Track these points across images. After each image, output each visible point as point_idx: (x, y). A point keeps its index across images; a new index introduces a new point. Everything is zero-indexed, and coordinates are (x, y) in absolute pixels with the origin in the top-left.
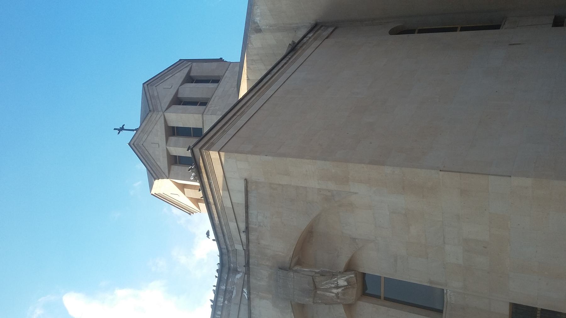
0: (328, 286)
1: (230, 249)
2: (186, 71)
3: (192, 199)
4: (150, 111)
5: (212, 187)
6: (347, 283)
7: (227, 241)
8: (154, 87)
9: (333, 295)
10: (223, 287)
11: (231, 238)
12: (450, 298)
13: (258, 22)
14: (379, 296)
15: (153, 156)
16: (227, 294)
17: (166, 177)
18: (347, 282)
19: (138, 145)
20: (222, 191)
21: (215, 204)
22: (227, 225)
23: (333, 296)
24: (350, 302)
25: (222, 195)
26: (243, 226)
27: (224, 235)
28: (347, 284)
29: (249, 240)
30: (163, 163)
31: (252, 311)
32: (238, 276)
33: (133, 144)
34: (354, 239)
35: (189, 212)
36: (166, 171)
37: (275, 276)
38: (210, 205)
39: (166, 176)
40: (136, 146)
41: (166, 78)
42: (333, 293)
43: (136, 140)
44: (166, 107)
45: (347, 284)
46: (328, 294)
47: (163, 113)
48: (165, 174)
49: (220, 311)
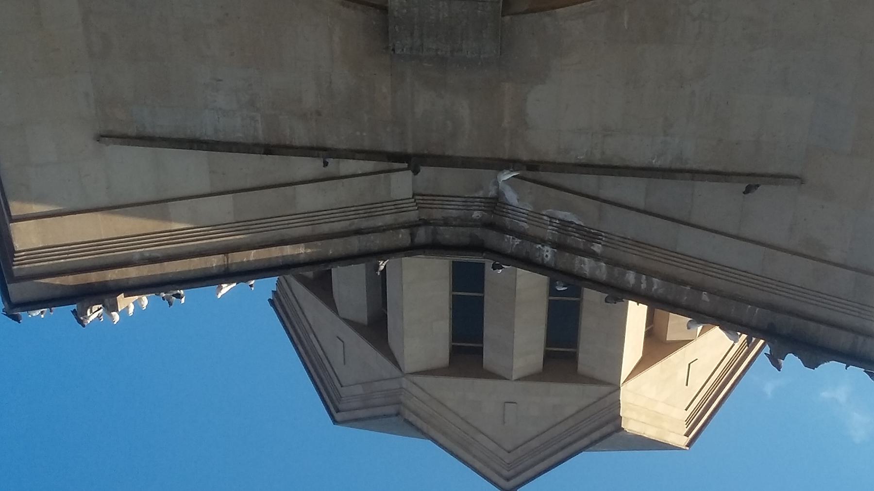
1: (413, 215)
5: (158, 255)
7: (379, 222)
20: (170, 220)
21: (226, 250)
22: (311, 216)
25: (188, 223)
26: (308, 166)
27: (358, 232)
32: (511, 196)
38: (234, 268)
49: (624, 275)
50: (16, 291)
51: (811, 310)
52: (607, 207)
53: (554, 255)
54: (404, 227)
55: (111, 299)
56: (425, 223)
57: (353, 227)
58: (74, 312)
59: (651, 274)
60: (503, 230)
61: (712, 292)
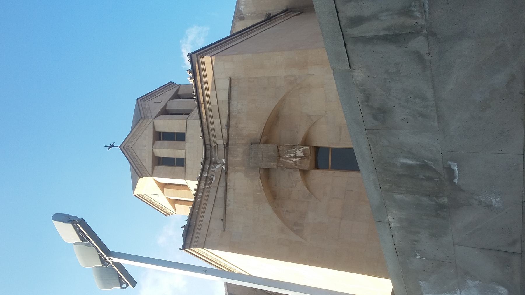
1: (213, 144)
2: (175, 90)
3: (169, 200)
4: (142, 118)
6: (304, 154)
7: (211, 137)
8: (146, 102)
9: (293, 162)
10: (205, 175)
11: (214, 135)
13: (242, 10)
15: (139, 157)
16: (208, 180)
17: (149, 176)
19: (127, 148)
21: (204, 103)
22: (212, 122)
23: (292, 163)
24: (304, 169)
26: (224, 122)
27: (209, 132)
29: (230, 126)
30: (148, 163)
31: (228, 184)
32: (218, 167)
33: (123, 147)
34: (310, 116)
35: (165, 214)
36: (150, 170)
37: (248, 151)
38: (200, 105)
39: (150, 175)
40: (126, 148)
41: (157, 95)
42: (292, 161)
43: (126, 144)
44: (156, 115)
46: (288, 161)
47: (153, 119)
48: (149, 173)
49: (201, 192)
50: (194, 56)
51: (195, 234)
53: (205, 176)
54: (210, 142)
55: (193, 78)
56: (211, 147)
57: (210, 131)
58: (190, 70)
59: (202, 198)
60: (210, 165)
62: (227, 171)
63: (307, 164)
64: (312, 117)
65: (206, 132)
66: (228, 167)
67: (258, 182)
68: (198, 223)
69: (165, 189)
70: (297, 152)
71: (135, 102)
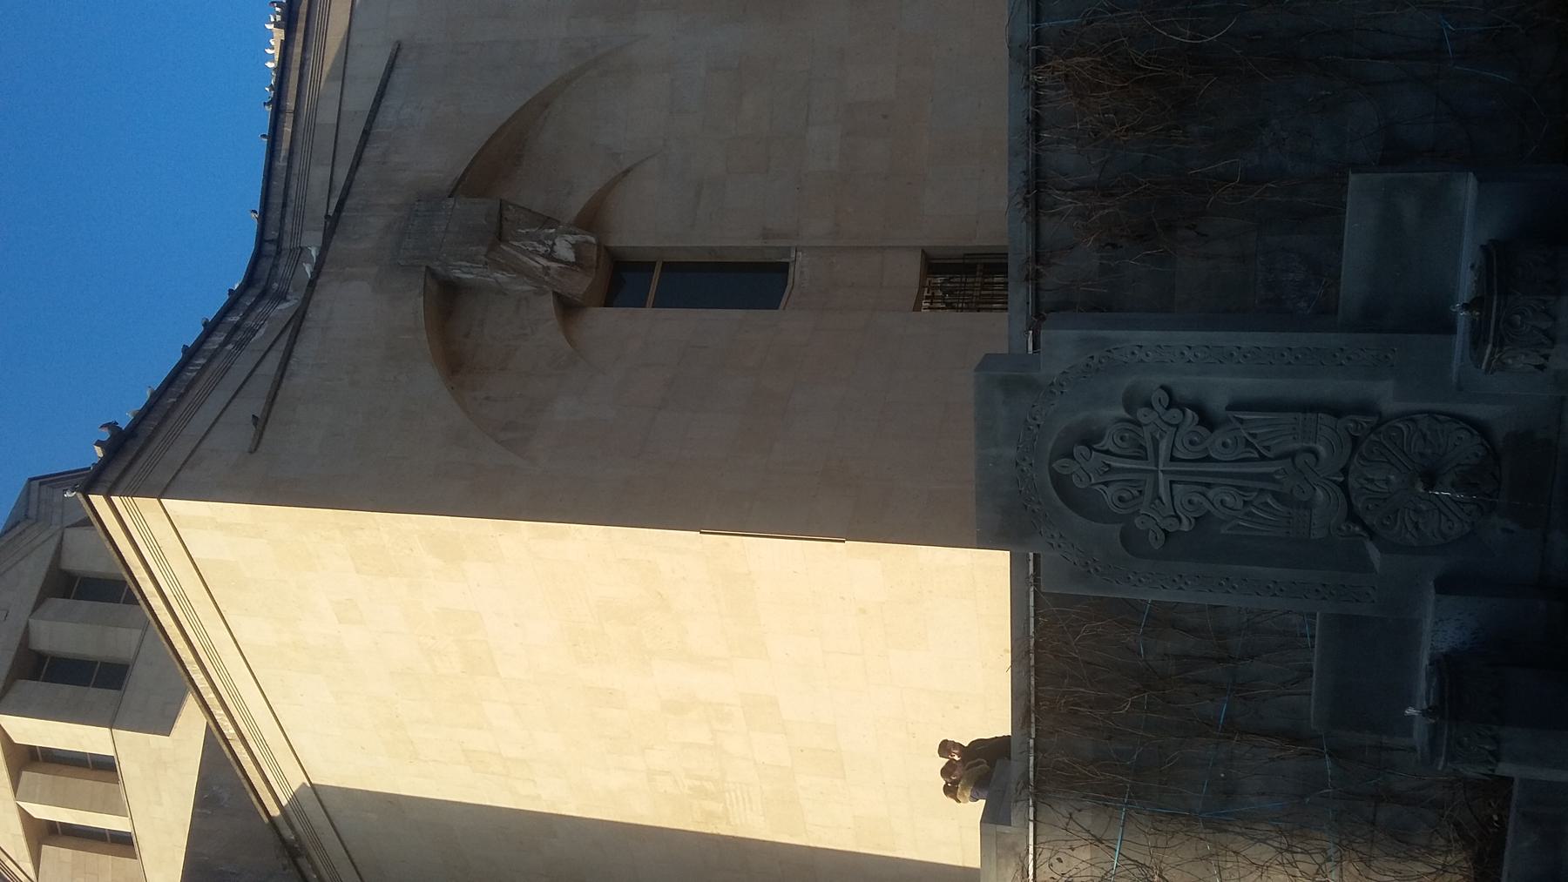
0: (532, 246)
1: (286, 244)
6: (576, 257)
7: (288, 220)
10: (235, 319)
12: (802, 273)
14: (645, 304)
18: (575, 253)
21: (296, 112)
23: (536, 267)
27: (284, 205)
28: (574, 260)
32: (284, 306)
45: (574, 260)
46: (525, 259)
49: (204, 358)
52: (262, 353)
56: (279, 253)
61: (175, 406)
62: (317, 277)
63: (579, 284)
64: (622, 157)
65: (276, 200)
66: (324, 267)
67: (413, 306)
68: (160, 437)
69: (25, 775)
70: (557, 241)
71: (24, 481)
